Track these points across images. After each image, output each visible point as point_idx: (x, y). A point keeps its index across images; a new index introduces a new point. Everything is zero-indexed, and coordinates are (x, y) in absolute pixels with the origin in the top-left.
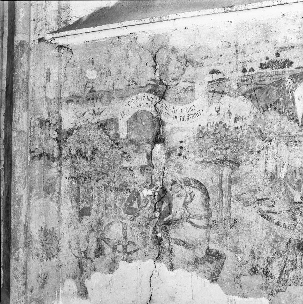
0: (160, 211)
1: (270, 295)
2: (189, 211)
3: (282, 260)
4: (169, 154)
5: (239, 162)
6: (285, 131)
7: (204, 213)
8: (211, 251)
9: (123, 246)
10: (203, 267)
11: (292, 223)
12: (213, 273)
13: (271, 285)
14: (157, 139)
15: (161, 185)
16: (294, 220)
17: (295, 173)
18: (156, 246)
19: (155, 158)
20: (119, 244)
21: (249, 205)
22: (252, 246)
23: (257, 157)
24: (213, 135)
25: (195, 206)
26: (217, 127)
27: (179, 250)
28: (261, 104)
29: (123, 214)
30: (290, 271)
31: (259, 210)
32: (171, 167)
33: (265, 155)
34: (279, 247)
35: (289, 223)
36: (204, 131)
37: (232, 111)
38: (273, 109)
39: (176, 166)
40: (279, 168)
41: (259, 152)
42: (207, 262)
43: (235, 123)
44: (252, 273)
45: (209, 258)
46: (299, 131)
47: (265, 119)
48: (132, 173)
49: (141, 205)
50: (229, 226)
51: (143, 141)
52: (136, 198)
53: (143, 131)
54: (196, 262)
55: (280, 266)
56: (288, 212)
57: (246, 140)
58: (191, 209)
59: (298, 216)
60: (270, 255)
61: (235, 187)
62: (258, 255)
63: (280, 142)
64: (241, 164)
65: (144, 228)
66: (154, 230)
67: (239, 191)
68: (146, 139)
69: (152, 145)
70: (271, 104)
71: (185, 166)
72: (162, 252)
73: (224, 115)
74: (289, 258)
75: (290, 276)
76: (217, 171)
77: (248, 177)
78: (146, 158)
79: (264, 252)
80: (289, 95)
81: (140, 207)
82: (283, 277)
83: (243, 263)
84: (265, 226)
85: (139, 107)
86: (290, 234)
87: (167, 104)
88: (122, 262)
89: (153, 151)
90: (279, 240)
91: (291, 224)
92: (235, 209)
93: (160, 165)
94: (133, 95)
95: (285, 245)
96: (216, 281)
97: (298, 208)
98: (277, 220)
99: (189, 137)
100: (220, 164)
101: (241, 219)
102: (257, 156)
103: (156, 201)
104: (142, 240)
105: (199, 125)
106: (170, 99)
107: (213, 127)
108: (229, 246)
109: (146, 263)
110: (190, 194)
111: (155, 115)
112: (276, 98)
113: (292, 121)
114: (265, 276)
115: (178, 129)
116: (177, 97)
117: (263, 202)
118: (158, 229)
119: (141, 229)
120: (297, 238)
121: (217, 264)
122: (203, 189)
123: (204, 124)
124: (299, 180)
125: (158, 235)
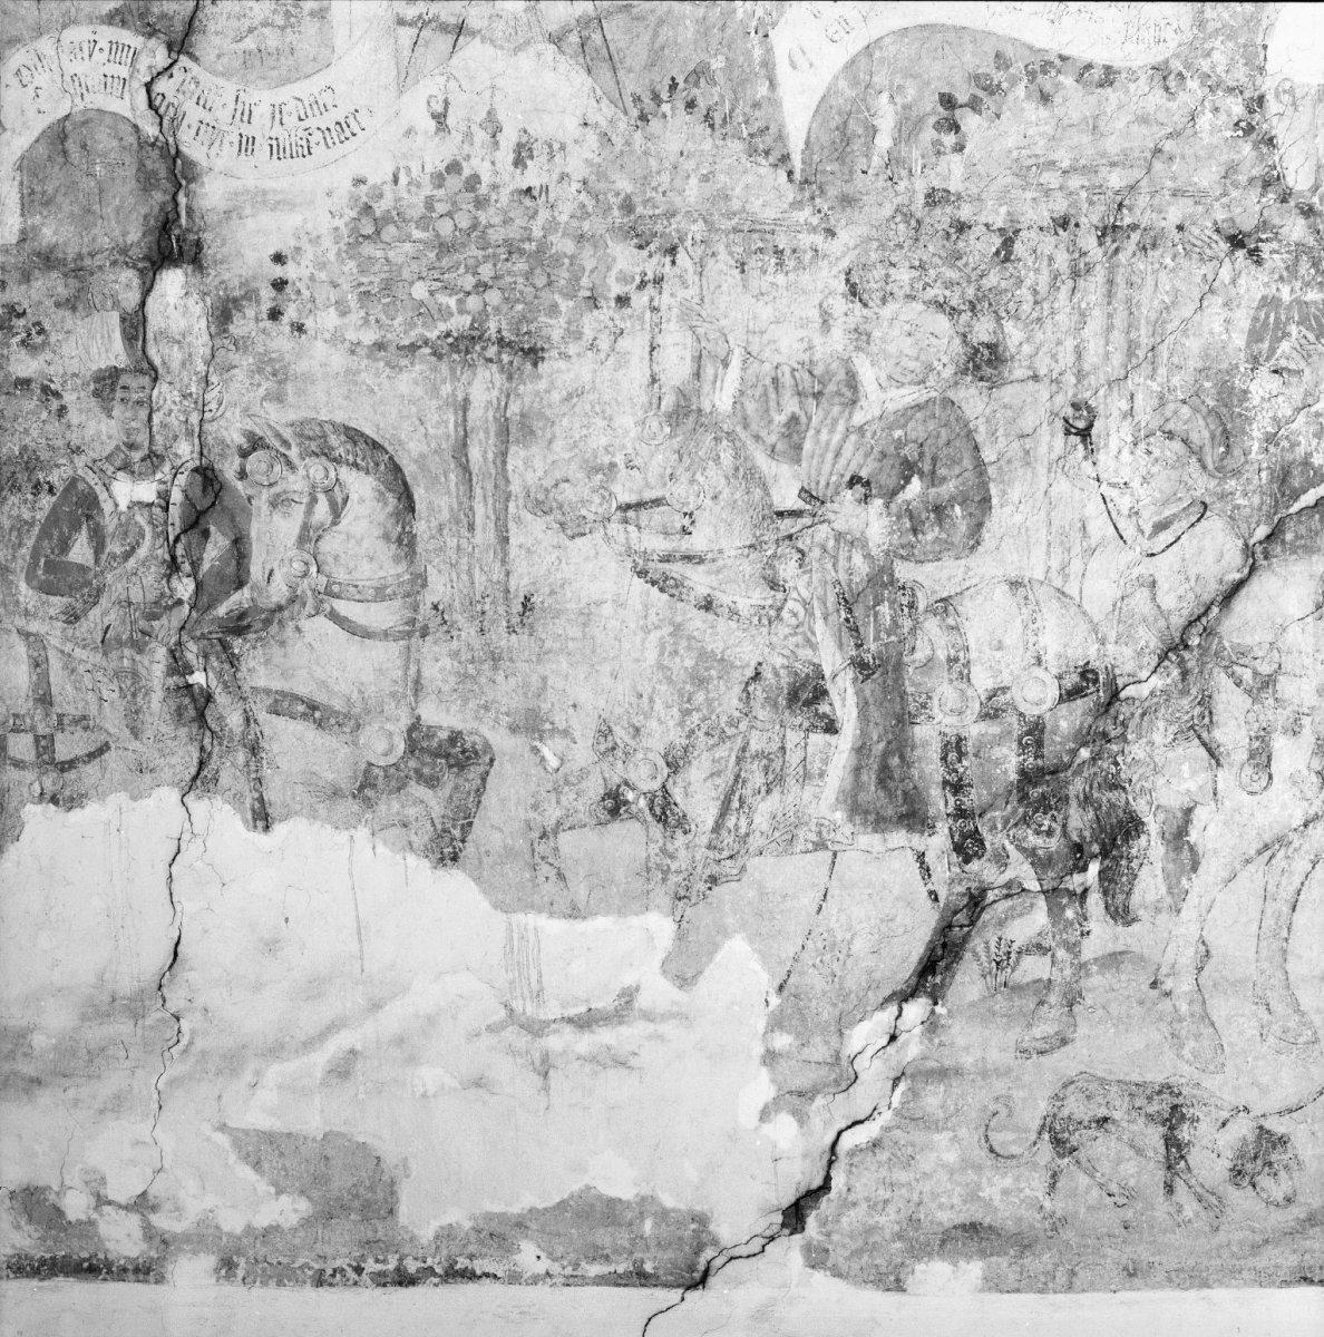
0: (194, 574)
1: (680, 899)
2: (326, 568)
3: (727, 752)
4: (223, 314)
5: (539, 346)
6: (736, 205)
7: (392, 572)
8: (429, 736)
9: (37, 739)
10: (396, 806)
11: (765, 599)
12: (439, 827)
13: (682, 862)
14: (163, 244)
15: (196, 455)
16: (772, 588)
17: (776, 389)
18: (186, 729)
19: (162, 334)
20: (16, 730)
21: (587, 531)
22: (602, 703)
23: (618, 323)
24: (424, 222)
25: (353, 541)
26: (440, 186)
27: (288, 739)
28: (631, 85)
29: (26, 593)
30: (759, 797)
31: (629, 552)
32: (236, 371)
33: (648, 314)
34: (713, 699)
35: (754, 602)
36: (380, 208)
37: (501, 116)
38: (681, 105)
39: (260, 371)
40: (709, 371)
41: (623, 301)
42: (412, 783)
43: (518, 171)
44: (604, 816)
45: (424, 764)
46: (791, 205)
47: (646, 153)
48: (55, 404)
49: (107, 551)
50: (505, 624)
51: (99, 256)
52: (84, 519)
53: (96, 207)
54: (367, 786)
55: (718, 781)
57: (568, 246)
58: (336, 558)
59: (788, 570)
60: (677, 737)
61: (522, 453)
62: (627, 739)
64: (546, 355)
65: (127, 652)
66: (174, 657)
67: (540, 473)
68: (113, 245)
69: (141, 271)
71: (301, 367)
72: (216, 749)
73: (468, 136)
74: (754, 746)
75: (758, 819)
76: (443, 387)
77: (577, 409)
78: (117, 335)
79: (653, 724)
80: (749, 45)
81: (104, 557)
82: (731, 822)
83: (566, 775)
84: (653, 618)
85: (72, 91)
87: (204, 77)
88: (39, 808)
89: (150, 301)
90: (713, 672)
91: (763, 603)
92: (528, 551)
93: (183, 364)
94: (39, 31)
95: (737, 689)
96: (455, 858)
97: (790, 537)
98: (702, 591)
99: (315, 234)
100: (455, 356)
101: (552, 593)
102: (616, 317)
103: (178, 531)
104: (121, 705)
105: (359, 181)
106: (219, 56)
107: (419, 186)
108: (504, 709)
109: (148, 803)
110: (328, 491)
111: (150, 130)
113: (764, 162)
114: (660, 826)
115: (262, 199)
116: (253, 46)
117: (644, 514)
118: (192, 652)
119: (114, 655)
121: (456, 788)
122: (382, 467)
123: (379, 174)
124: (794, 419)
125: (191, 679)
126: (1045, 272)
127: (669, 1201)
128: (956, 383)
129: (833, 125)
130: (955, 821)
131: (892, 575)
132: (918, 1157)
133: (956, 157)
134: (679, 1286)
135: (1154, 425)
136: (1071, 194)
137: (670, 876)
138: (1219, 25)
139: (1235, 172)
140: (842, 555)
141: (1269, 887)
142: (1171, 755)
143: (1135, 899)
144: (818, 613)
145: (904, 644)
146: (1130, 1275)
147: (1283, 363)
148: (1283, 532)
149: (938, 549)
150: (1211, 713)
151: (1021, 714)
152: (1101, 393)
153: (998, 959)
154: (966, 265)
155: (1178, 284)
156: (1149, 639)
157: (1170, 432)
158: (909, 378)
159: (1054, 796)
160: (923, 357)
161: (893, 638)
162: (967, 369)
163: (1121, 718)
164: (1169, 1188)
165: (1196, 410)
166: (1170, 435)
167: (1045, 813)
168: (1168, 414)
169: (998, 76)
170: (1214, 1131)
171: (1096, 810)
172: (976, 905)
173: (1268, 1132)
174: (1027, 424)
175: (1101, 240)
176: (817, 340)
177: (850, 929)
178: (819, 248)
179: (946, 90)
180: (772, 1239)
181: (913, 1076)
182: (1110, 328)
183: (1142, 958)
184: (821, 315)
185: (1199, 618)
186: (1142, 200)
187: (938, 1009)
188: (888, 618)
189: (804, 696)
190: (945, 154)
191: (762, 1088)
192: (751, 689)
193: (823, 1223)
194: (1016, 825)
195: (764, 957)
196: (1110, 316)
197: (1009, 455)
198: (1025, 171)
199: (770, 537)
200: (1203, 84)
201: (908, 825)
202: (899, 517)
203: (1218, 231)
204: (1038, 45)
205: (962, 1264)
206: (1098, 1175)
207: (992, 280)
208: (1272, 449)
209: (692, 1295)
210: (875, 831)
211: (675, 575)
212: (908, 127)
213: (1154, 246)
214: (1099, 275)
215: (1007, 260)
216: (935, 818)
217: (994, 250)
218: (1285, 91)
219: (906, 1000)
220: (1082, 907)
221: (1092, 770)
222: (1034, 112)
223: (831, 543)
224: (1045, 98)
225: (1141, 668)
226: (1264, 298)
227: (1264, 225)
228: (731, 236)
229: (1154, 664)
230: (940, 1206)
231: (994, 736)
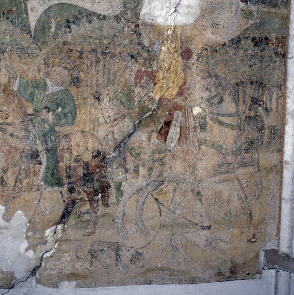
1: (6, 202)
6: (18, 42)
11: (25, 134)
13: (6, 193)
16: (27, 132)
17: (28, 85)
34: (13, 157)
35: (22, 135)
38: (5, 18)
46: (31, 43)
56: (21, 124)
59: (30, 127)
63: (13, 54)
70: (4, 14)
74: (23, 167)
75: (24, 184)
80: (22, 5)
86: (23, 145)
90: (13, 150)
91: (25, 135)
95: (19, 154)
97: (31, 120)
98: (10, 132)
112: (9, 7)
113: (25, 33)
114: (1, 185)
120: (30, 148)
126: (90, 61)
127: (5, 270)
128: (69, 86)
129: (41, 25)
130: (69, 185)
131: (54, 129)
132: (61, 259)
133: (70, 34)
134: (7, 288)
135: (114, 97)
136: (96, 44)
137: (4, 197)
138: (129, 8)
139: (132, 41)
140: (43, 124)
141: (138, 199)
142: (117, 170)
143: (109, 201)
144: (37, 137)
145: (57, 145)
146: (108, 283)
147: (142, 84)
148: (142, 122)
149: (65, 123)
150: (126, 161)
151: (84, 161)
152: (102, 89)
153: (79, 215)
154: (72, 59)
155: (119, 65)
156: (112, 144)
157: (117, 99)
158: (58, 85)
159: (91, 179)
160: (62, 80)
161: (55, 144)
162: (72, 83)
163: (106, 162)
164: (117, 265)
165: (123, 94)
166: (117, 100)
167: (89, 183)
168: (117, 95)
169: (79, 16)
170: (126, 252)
171: (100, 182)
172: (74, 203)
173: (138, 252)
174: (86, 95)
175: (102, 55)
176: (37, 75)
177: (45, 208)
178: (38, 53)
179: (67, 19)
180: (28, 277)
181: (60, 241)
182: (104, 75)
183: (110, 215)
184: (38, 69)
185: (123, 141)
186: (112, 46)
187: (66, 226)
188: (53, 139)
189: (34, 156)
190: (67, 33)
191: (25, 244)
192: (22, 154)
193: (40, 274)
194: (82, 185)
195: (26, 215)
196: (104, 72)
197: (81, 103)
198: (85, 38)
199: (26, 120)
200: (125, 21)
201: (58, 185)
202: (56, 116)
203: (128, 54)
204: (88, 9)
205: (71, 282)
206: (101, 262)
207: (78, 63)
208: (140, 104)
209: (10, 290)
210: (51, 187)
211: (4, 128)
212: (58, 26)
213: (114, 57)
214: (102, 63)
215: (81, 58)
216: (65, 184)
217: (78, 56)
218: (144, 24)
219: (58, 224)
220: (97, 204)
221: (99, 174)
222: (88, 25)
223: (40, 122)
224: (90, 22)
225: (110, 151)
226: (138, 70)
227: (138, 53)
228: (17, 50)
229: (113, 150)
230: (66, 270)
231: (78, 166)
